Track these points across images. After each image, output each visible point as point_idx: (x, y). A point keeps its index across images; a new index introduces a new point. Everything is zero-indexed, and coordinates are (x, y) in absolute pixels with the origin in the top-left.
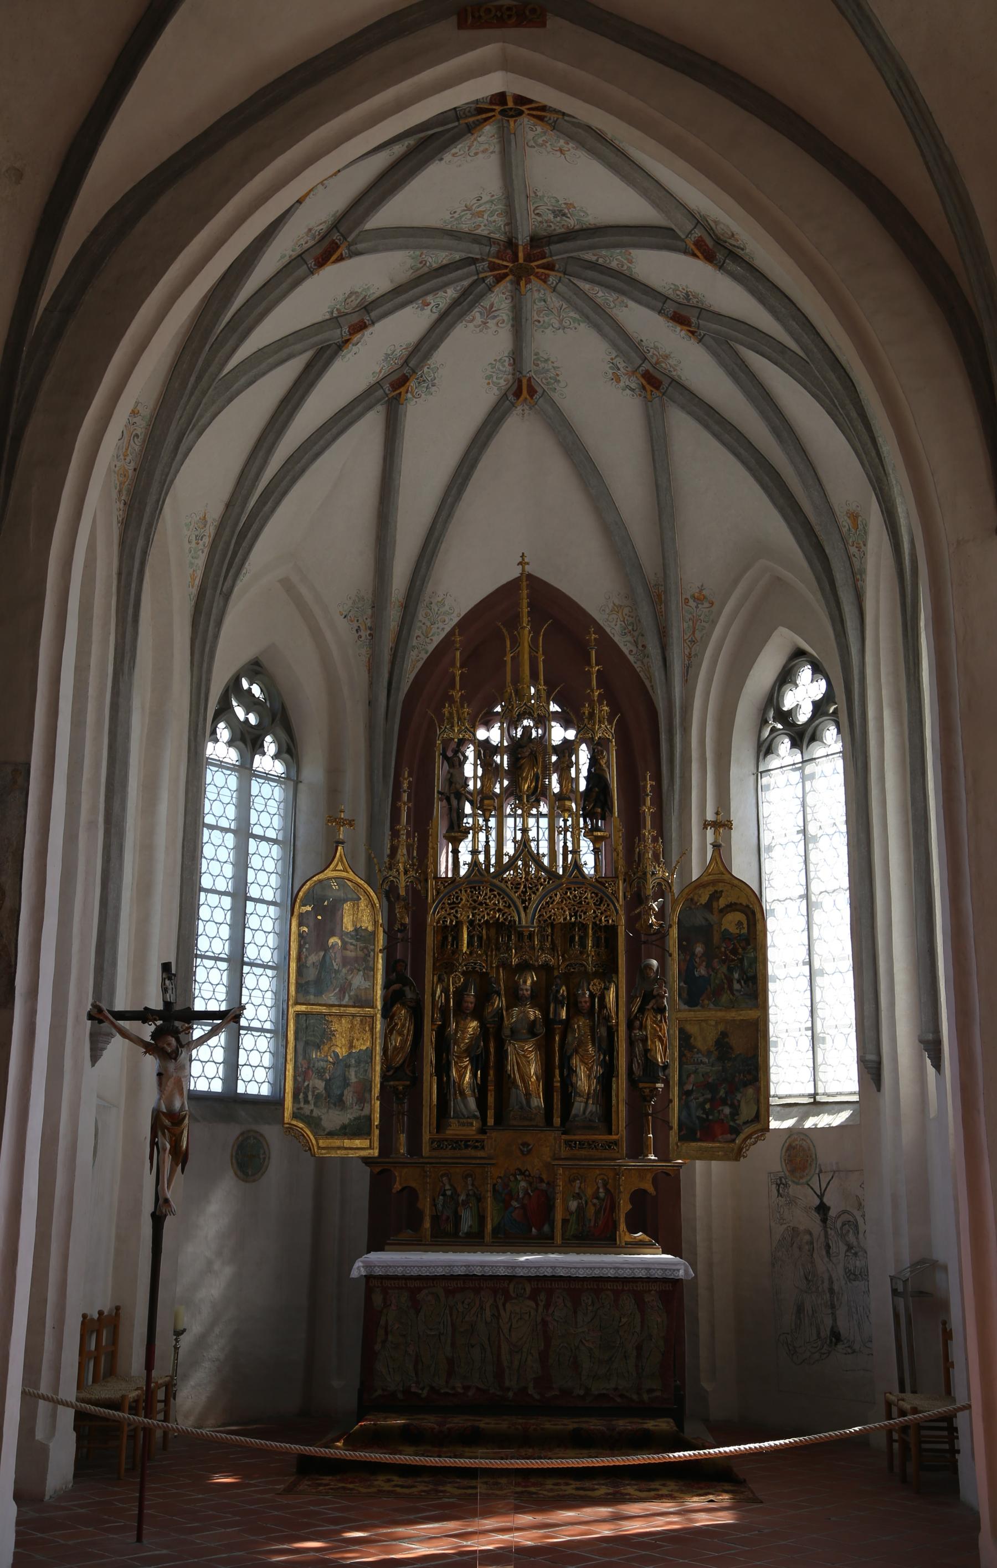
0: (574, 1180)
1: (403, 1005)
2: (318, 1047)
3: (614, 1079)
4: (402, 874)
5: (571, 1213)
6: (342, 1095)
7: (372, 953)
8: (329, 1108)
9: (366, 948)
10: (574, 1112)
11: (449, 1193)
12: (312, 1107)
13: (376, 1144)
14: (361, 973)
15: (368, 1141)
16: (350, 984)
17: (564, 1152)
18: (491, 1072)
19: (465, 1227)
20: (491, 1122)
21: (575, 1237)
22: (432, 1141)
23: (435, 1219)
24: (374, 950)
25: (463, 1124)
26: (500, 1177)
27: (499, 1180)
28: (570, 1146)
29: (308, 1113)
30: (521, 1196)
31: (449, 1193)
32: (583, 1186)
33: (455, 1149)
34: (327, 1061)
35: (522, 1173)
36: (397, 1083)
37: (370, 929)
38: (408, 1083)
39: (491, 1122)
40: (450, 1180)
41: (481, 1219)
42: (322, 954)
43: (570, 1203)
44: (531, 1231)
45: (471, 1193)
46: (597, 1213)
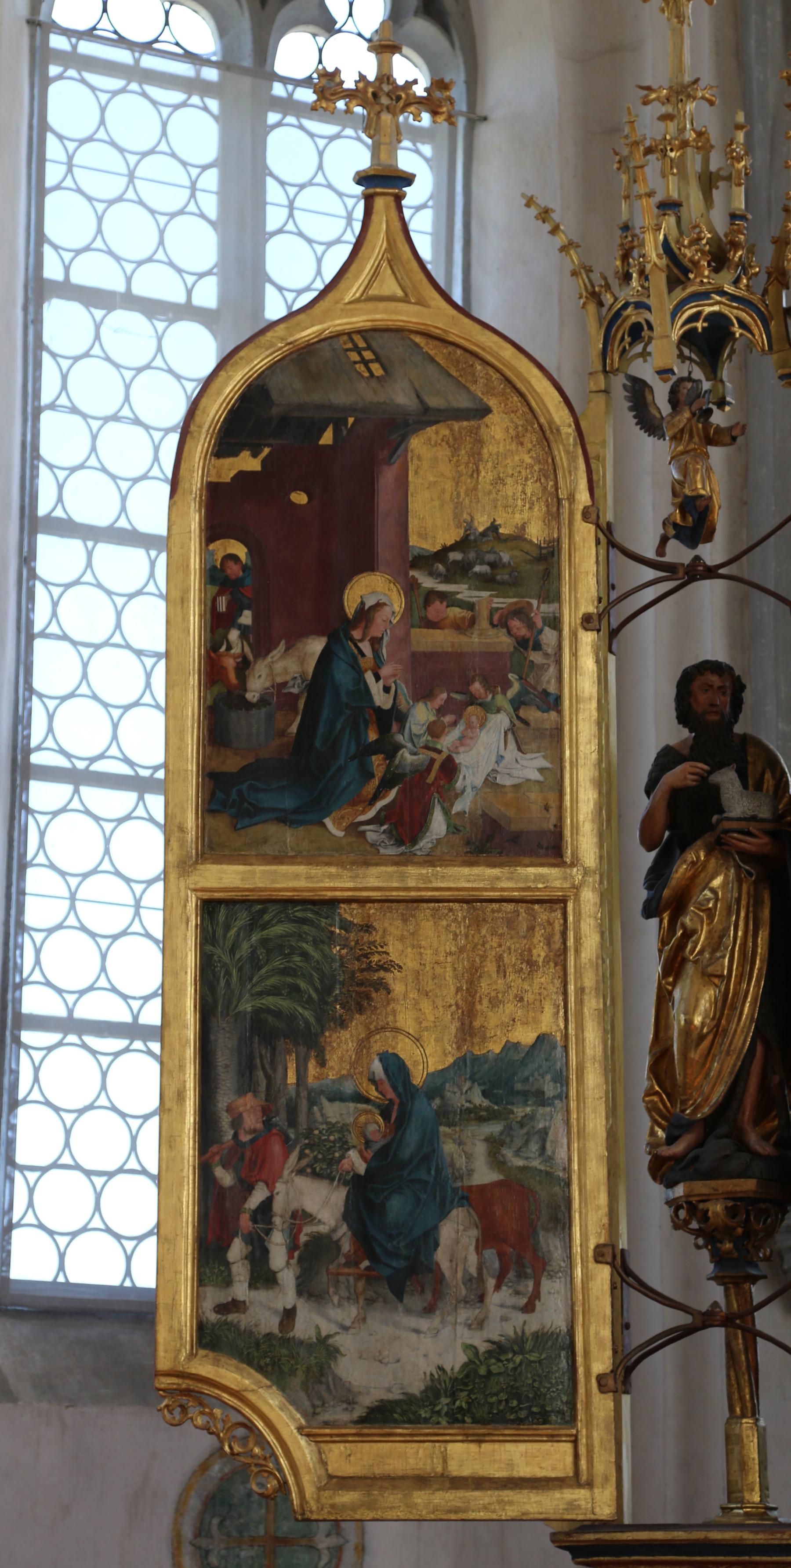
1: (719, 847)
2: (311, 1043)
4: (659, 281)
6: (430, 1238)
7: (548, 636)
8: (370, 1302)
9: (520, 612)
12: (287, 1294)
13: (603, 1463)
14: (500, 721)
15: (567, 1448)
16: (450, 769)
24: (555, 623)
29: (270, 1323)
34: (359, 1098)
36: (701, 1187)
37: (536, 532)
38: (749, 1185)
42: (316, 646)
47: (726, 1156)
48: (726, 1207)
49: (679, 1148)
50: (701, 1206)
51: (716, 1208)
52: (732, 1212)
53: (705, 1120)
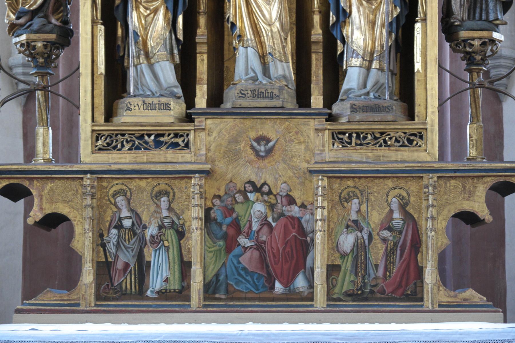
0: (348, 200)
3: (418, 26)
5: (344, 256)
10: (345, 86)
11: (127, 223)
17: (332, 153)
18: (202, 21)
19: (156, 282)
20: (201, 101)
21: (351, 295)
22: (97, 136)
23: (104, 269)
25: (151, 107)
26: (219, 197)
27: (217, 202)
28: (341, 140)
30: (255, 227)
31: (127, 223)
32: (364, 208)
33: (138, 148)
35: (257, 189)
36: (33, 36)
38: (53, 37)
39: (201, 101)
40: (129, 201)
41: (185, 267)
43: (342, 238)
44: (273, 287)
45: (167, 222)
46: (389, 254)
47: (44, 25)
48: (44, 45)
49: (22, 21)
50: (33, 44)
51: (39, 44)
52: (45, 46)
53: (33, 11)
